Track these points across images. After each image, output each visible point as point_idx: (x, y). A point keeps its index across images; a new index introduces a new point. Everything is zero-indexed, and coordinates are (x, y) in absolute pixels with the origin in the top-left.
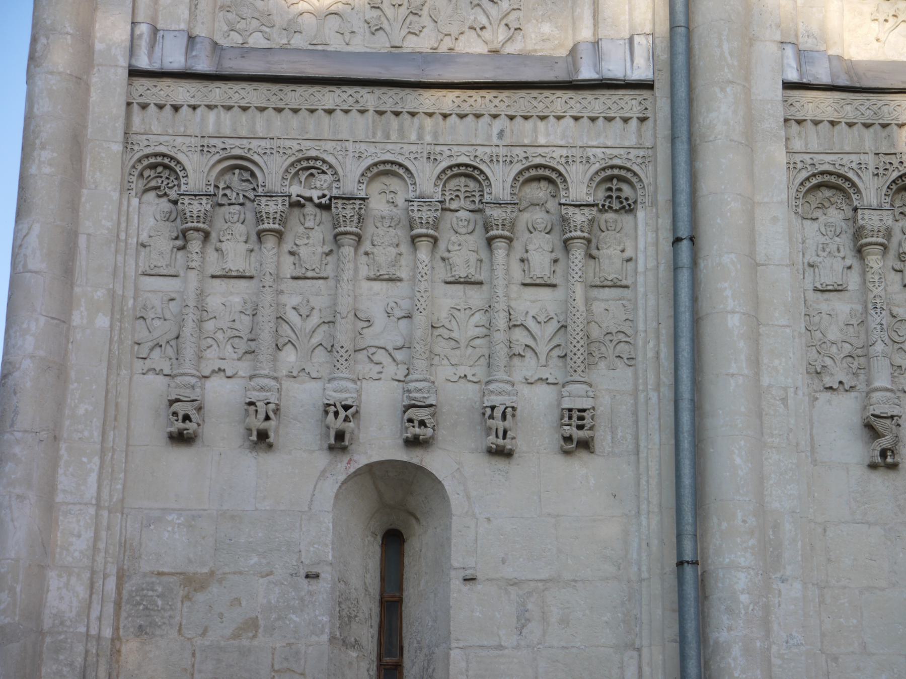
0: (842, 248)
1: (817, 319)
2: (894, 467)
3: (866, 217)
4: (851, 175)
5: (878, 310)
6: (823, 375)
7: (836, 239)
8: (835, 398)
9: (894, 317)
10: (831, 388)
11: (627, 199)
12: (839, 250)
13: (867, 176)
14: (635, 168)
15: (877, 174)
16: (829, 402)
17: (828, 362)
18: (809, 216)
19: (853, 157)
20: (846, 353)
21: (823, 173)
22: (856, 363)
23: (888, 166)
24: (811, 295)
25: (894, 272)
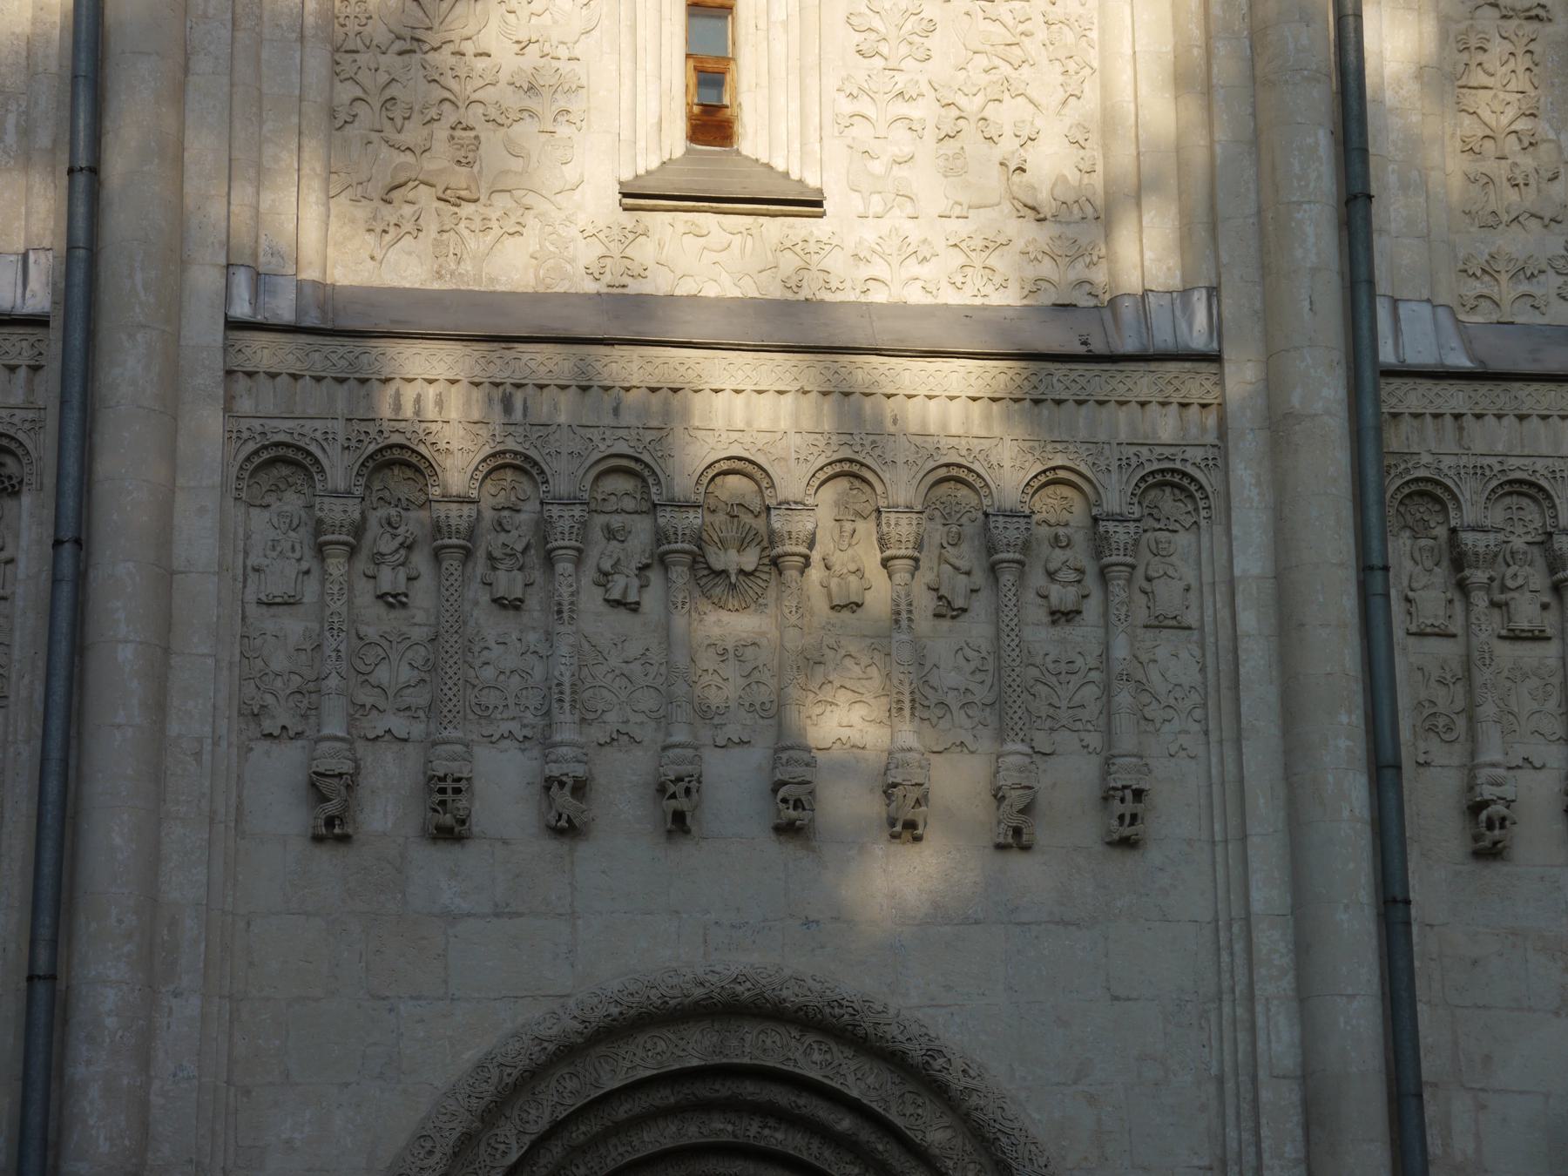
0: (298, 547)
1: (258, 642)
2: (345, 839)
3: (326, 507)
4: (313, 448)
7: (292, 534)
10: (270, 735)
11: (10, 478)
12: (293, 549)
13: (335, 450)
14: (21, 436)
17: (269, 699)
18: (258, 502)
19: (318, 424)
20: (293, 687)
21: (277, 445)
24: (252, 609)
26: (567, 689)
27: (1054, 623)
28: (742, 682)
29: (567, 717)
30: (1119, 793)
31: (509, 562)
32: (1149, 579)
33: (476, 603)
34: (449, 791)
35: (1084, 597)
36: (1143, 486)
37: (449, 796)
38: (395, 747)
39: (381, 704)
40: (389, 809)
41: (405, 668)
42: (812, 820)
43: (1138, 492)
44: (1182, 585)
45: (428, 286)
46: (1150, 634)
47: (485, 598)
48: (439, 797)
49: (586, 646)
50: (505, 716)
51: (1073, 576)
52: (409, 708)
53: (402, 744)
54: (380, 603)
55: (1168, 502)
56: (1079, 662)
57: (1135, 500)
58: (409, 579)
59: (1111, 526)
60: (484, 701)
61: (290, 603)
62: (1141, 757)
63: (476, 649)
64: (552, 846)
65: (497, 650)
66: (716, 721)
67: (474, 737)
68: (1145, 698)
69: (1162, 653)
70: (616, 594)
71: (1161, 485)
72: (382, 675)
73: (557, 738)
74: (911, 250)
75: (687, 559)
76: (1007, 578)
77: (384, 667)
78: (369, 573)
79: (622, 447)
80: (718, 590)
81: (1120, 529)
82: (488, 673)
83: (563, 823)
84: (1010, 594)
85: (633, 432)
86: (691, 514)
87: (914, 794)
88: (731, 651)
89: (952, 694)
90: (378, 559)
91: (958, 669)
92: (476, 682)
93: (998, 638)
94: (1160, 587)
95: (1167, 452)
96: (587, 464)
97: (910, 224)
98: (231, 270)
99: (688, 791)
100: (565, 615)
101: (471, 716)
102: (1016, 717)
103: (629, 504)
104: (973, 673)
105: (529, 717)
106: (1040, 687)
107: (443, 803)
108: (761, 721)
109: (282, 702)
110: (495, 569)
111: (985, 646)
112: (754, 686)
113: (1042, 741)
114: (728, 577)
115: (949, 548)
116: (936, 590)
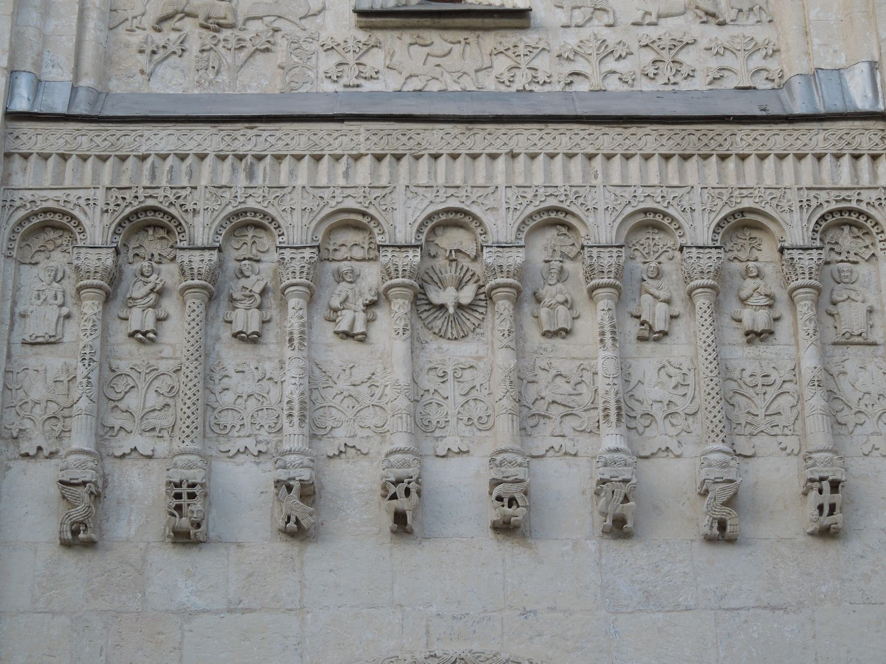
0: (60, 296)
1: (22, 375)
2: (90, 544)
3: (82, 256)
4: (76, 212)
5: (86, 362)
6: (20, 440)
7: (55, 284)
8: (32, 467)
9: (113, 371)
10: (27, 455)
12: (56, 297)
15: (107, 211)
16: (24, 471)
17: (28, 424)
18: (28, 261)
19: (81, 193)
20: (50, 413)
21: (46, 211)
22: (60, 425)
23: (120, 201)
25: (119, 321)
28: (462, 400)
29: (296, 429)
30: (816, 485)
31: (247, 302)
32: (834, 303)
34: (185, 496)
35: (776, 320)
36: (824, 224)
37: (185, 501)
38: (142, 462)
41: (152, 395)
42: (527, 518)
43: (820, 229)
44: (864, 308)
45: (190, 92)
46: (839, 350)
49: (317, 372)
50: (242, 433)
51: (764, 301)
52: (153, 429)
53: (146, 461)
54: (132, 340)
55: (846, 239)
56: (774, 376)
57: (818, 236)
58: (159, 320)
59: (795, 254)
61: (51, 342)
62: (836, 453)
63: (217, 377)
64: (283, 547)
65: (236, 378)
66: (438, 433)
67: (214, 453)
68: (838, 405)
69: (851, 366)
70: (344, 326)
71: (840, 225)
73: (286, 447)
74: (609, 50)
75: (409, 293)
78: (123, 315)
80: (438, 323)
81: (805, 256)
83: (292, 525)
84: (706, 316)
86: (411, 253)
88: (450, 373)
89: (656, 406)
92: (215, 405)
94: (843, 309)
95: (844, 194)
96: (319, 218)
97: (605, 33)
98: (15, 75)
99: (407, 492)
101: (210, 435)
103: (358, 253)
104: (675, 387)
105: (264, 434)
106: (738, 398)
107: (179, 508)
108: (478, 433)
109: (40, 426)
110: (235, 308)
112: (472, 403)
113: (744, 445)
114: (447, 310)
115: (649, 281)
116: (639, 317)
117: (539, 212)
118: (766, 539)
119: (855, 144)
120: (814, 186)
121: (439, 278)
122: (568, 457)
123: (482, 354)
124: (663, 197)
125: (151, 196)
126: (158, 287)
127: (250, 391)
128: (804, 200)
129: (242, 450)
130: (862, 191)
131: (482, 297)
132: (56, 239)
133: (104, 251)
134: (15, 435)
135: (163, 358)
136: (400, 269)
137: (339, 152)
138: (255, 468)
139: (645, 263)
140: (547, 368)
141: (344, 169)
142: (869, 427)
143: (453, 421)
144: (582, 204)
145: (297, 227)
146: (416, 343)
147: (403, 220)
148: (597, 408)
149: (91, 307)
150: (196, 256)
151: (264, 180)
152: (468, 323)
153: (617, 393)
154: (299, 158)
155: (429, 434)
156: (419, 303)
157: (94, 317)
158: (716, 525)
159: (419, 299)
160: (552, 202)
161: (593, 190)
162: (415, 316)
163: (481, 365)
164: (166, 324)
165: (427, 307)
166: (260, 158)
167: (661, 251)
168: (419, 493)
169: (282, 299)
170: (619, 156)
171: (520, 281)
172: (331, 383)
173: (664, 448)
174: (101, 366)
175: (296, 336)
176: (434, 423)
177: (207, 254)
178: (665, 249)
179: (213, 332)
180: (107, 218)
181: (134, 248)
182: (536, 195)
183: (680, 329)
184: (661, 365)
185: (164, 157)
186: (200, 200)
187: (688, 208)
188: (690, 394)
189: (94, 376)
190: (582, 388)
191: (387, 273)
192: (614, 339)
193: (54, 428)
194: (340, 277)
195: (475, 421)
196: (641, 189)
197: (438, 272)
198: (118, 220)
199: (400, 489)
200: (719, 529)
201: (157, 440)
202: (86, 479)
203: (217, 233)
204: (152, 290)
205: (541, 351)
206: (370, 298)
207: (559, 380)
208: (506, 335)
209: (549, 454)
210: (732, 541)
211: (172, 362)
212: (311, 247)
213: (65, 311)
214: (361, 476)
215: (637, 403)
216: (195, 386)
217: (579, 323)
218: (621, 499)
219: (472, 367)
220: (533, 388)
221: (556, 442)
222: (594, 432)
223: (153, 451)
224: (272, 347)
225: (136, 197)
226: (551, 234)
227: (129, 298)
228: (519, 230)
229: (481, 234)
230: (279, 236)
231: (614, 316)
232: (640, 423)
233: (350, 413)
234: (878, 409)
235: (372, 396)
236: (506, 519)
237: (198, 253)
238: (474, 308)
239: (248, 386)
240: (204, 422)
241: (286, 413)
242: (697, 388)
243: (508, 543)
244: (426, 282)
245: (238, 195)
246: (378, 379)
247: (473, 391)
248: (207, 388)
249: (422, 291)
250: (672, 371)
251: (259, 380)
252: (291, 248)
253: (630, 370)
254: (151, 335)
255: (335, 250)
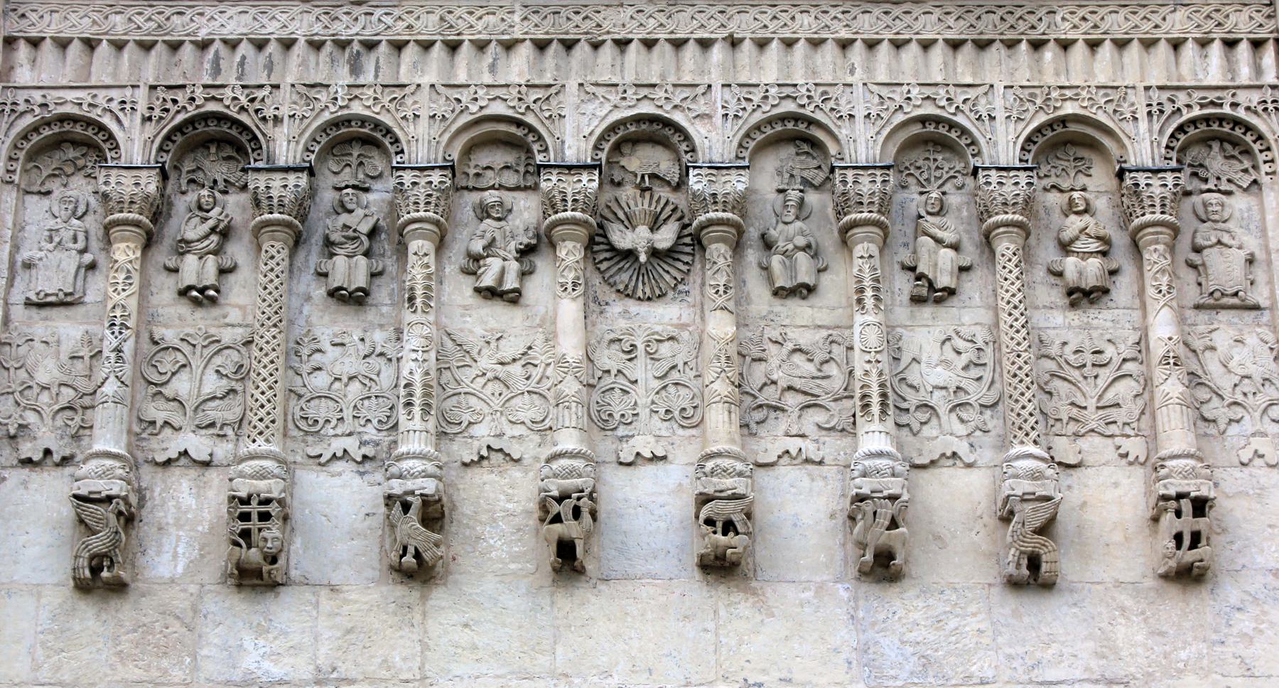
2: (119, 587)
3: (113, 180)
4: (107, 121)
5: (116, 329)
6: (19, 440)
9: (156, 343)
12: (75, 240)
15: (150, 119)
16: (25, 484)
17: (31, 417)
18: (35, 189)
19: (114, 93)
20: (63, 402)
21: (63, 119)
22: (78, 418)
23: (169, 105)
24: (18, 312)
25: (165, 273)
26: (418, 391)
27: (1073, 305)
28: (657, 384)
29: (417, 423)
30: (1173, 504)
31: (350, 247)
32: (1198, 250)
33: (308, 298)
34: (255, 517)
35: (1113, 273)
36: (1182, 137)
37: (254, 524)
38: (193, 473)
39: (176, 420)
40: (180, 550)
41: (211, 377)
42: (749, 551)
43: (1177, 145)
44: (1242, 254)
46: (1203, 316)
47: (319, 292)
48: (241, 526)
49: (449, 344)
50: (339, 431)
51: (1094, 246)
52: (212, 425)
53: (199, 470)
54: (184, 300)
55: (1216, 162)
56: (1110, 351)
57: (1174, 155)
58: (223, 272)
59: (1142, 178)
60: (311, 413)
61: (66, 302)
62: (1200, 459)
63: (305, 351)
66: (622, 431)
67: (299, 459)
68: (1203, 394)
69: (1222, 339)
70: (488, 280)
71: (1206, 141)
72: (182, 386)
73: (403, 449)
75: (582, 232)
76: (1005, 246)
77: (184, 375)
78: (171, 265)
79: (498, 109)
80: (625, 277)
81: (1156, 182)
82: (320, 381)
83: (409, 560)
84: (1010, 266)
85: (514, 92)
86: (585, 177)
87: (887, 510)
88: (641, 347)
89: (937, 394)
90: (183, 246)
91: (945, 363)
92: (302, 391)
93: (997, 325)
94: (1211, 256)
95: (1212, 96)
96: (454, 128)
99: (577, 513)
100: (418, 301)
101: (295, 433)
102: (1025, 413)
104: (966, 368)
105: (371, 432)
106: (1057, 383)
107: (246, 534)
108: (680, 432)
109: (48, 420)
110: (332, 255)
111: (981, 336)
112: (672, 389)
113: (1065, 450)
114: (637, 259)
115: (929, 218)
116: (913, 269)
117: (770, 121)
118: (1098, 583)
119: (1228, 25)
120: (1169, 84)
121: (625, 213)
122: (810, 467)
123: (690, 322)
124: (948, 99)
125: (214, 98)
126: (222, 226)
127: (352, 372)
128: (1154, 104)
129: (339, 454)
130: (1238, 92)
131: (688, 240)
132: (76, 158)
133: (144, 173)
134: (12, 432)
135: (228, 325)
136: (569, 199)
137: (483, 37)
138: (357, 480)
139: (922, 193)
140: (780, 339)
141: (491, 60)
142: (1248, 426)
143: (644, 413)
144: (832, 109)
145: (422, 141)
146: (592, 304)
147: (575, 131)
148: (852, 397)
149: (126, 252)
150: (277, 181)
151: (376, 76)
152: (667, 277)
153: (881, 374)
154: (427, 46)
155: (609, 433)
156: (596, 248)
157: (129, 266)
158: (1025, 562)
159: (597, 244)
160: (789, 107)
161: (848, 90)
162: (590, 267)
163: (685, 335)
164: (231, 278)
165: (607, 255)
166: (370, 46)
167: (945, 176)
168: (594, 514)
169: (400, 243)
170: (885, 43)
171: (741, 217)
172: (468, 361)
173: (949, 454)
174: (138, 336)
175: (419, 292)
176: (617, 416)
177: (292, 179)
178: (952, 173)
179: (302, 288)
180: (150, 129)
181: (188, 172)
182: (766, 98)
183: (973, 288)
184: (944, 337)
185: (232, 45)
186: (284, 103)
187: (984, 114)
188: (987, 375)
189: (128, 348)
190: (832, 369)
191: (551, 205)
192: (877, 298)
193: (69, 423)
194: (484, 212)
195: (676, 413)
196: (918, 89)
197: (624, 205)
198: (165, 131)
199: (565, 509)
200: (1029, 568)
201: (218, 440)
202: (113, 493)
203: (308, 150)
204: (213, 230)
205: (771, 316)
206: (526, 241)
207: (797, 358)
208: (721, 292)
209: (781, 461)
210: (1048, 586)
211: (240, 330)
212: (441, 168)
213: (88, 258)
214: (510, 491)
215: (909, 390)
216: (272, 362)
217: (826, 279)
218: (887, 523)
219: (671, 338)
220: (759, 369)
221: (793, 445)
222: (849, 430)
223: (211, 455)
224: (384, 309)
225: (193, 99)
226: (788, 151)
227: (180, 241)
228: (740, 145)
229: (686, 152)
230: (397, 153)
231: (878, 265)
232: (914, 419)
233: (496, 403)
234: (1262, 400)
235: (527, 379)
236: (720, 551)
237: (278, 176)
238: (676, 256)
239: (349, 364)
240: (286, 415)
241: (402, 400)
242: (998, 369)
243: (722, 588)
244: (607, 219)
245: (339, 96)
246: (538, 356)
247: (673, 372)
248: (291, 368)
249: (601, 232)
250: (961, 344)
251: (365, 357)
252: (412, 168)
253: (900, 344)
254: (212, 293)
255: (478, 175)
